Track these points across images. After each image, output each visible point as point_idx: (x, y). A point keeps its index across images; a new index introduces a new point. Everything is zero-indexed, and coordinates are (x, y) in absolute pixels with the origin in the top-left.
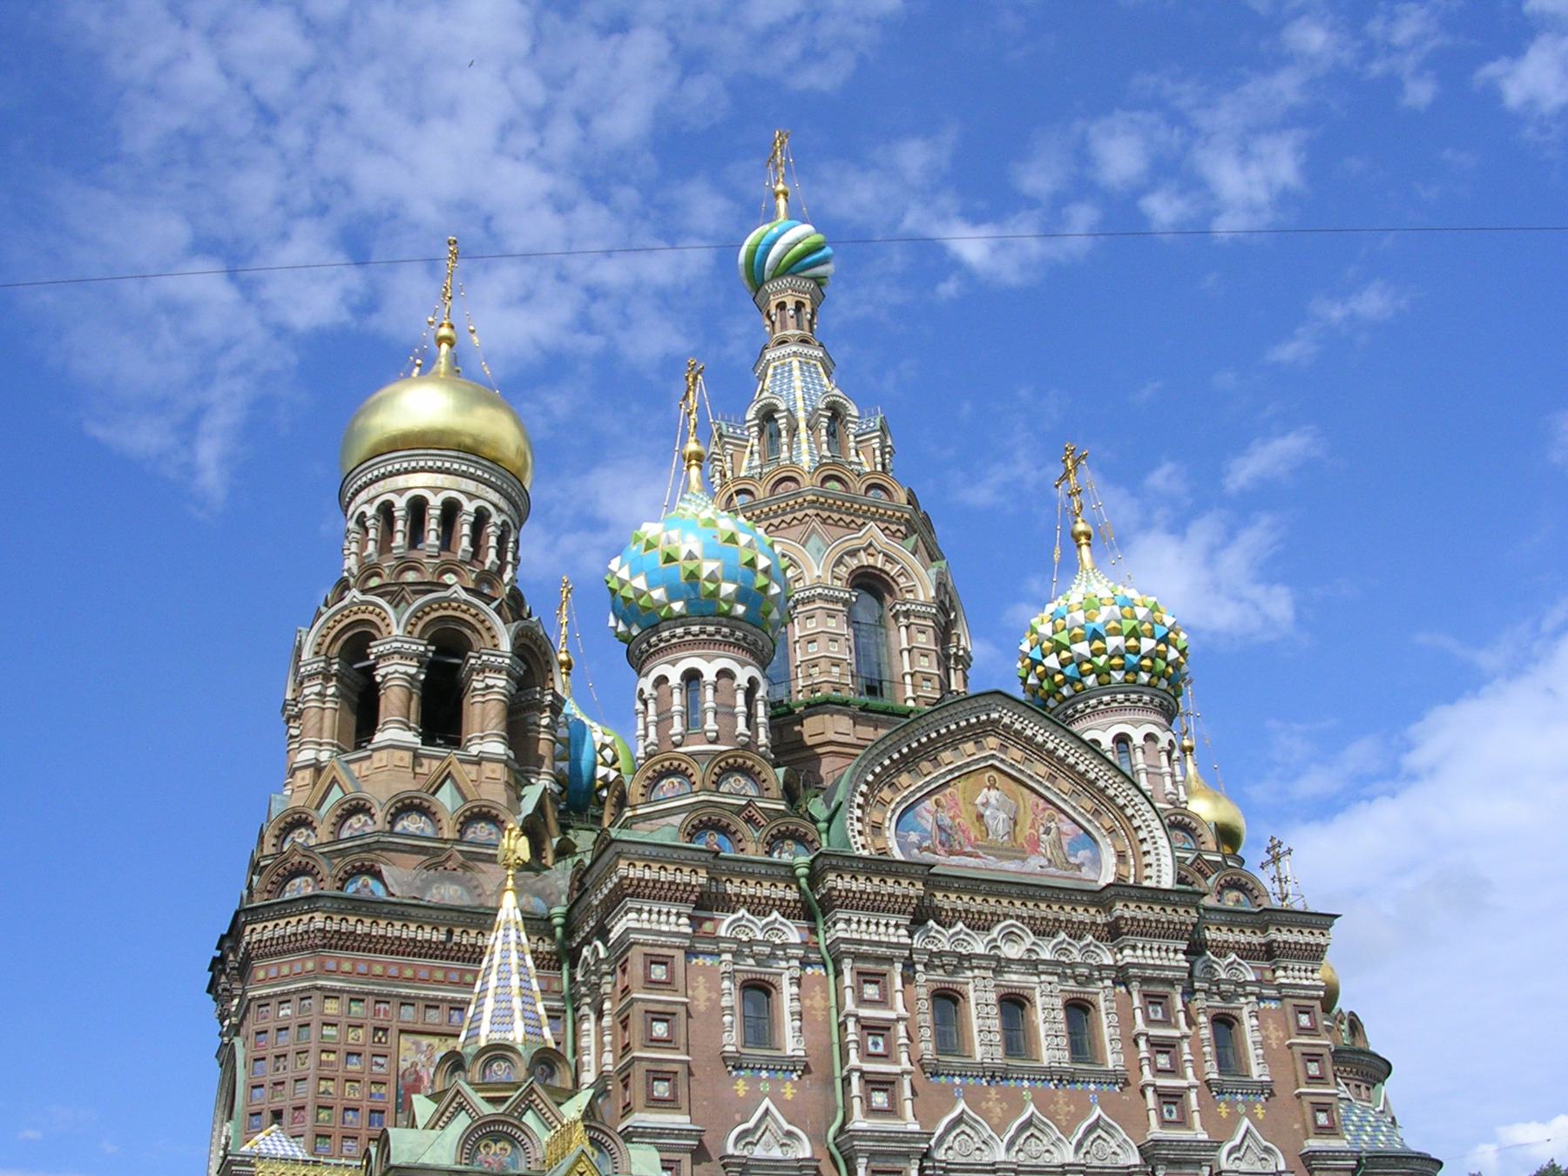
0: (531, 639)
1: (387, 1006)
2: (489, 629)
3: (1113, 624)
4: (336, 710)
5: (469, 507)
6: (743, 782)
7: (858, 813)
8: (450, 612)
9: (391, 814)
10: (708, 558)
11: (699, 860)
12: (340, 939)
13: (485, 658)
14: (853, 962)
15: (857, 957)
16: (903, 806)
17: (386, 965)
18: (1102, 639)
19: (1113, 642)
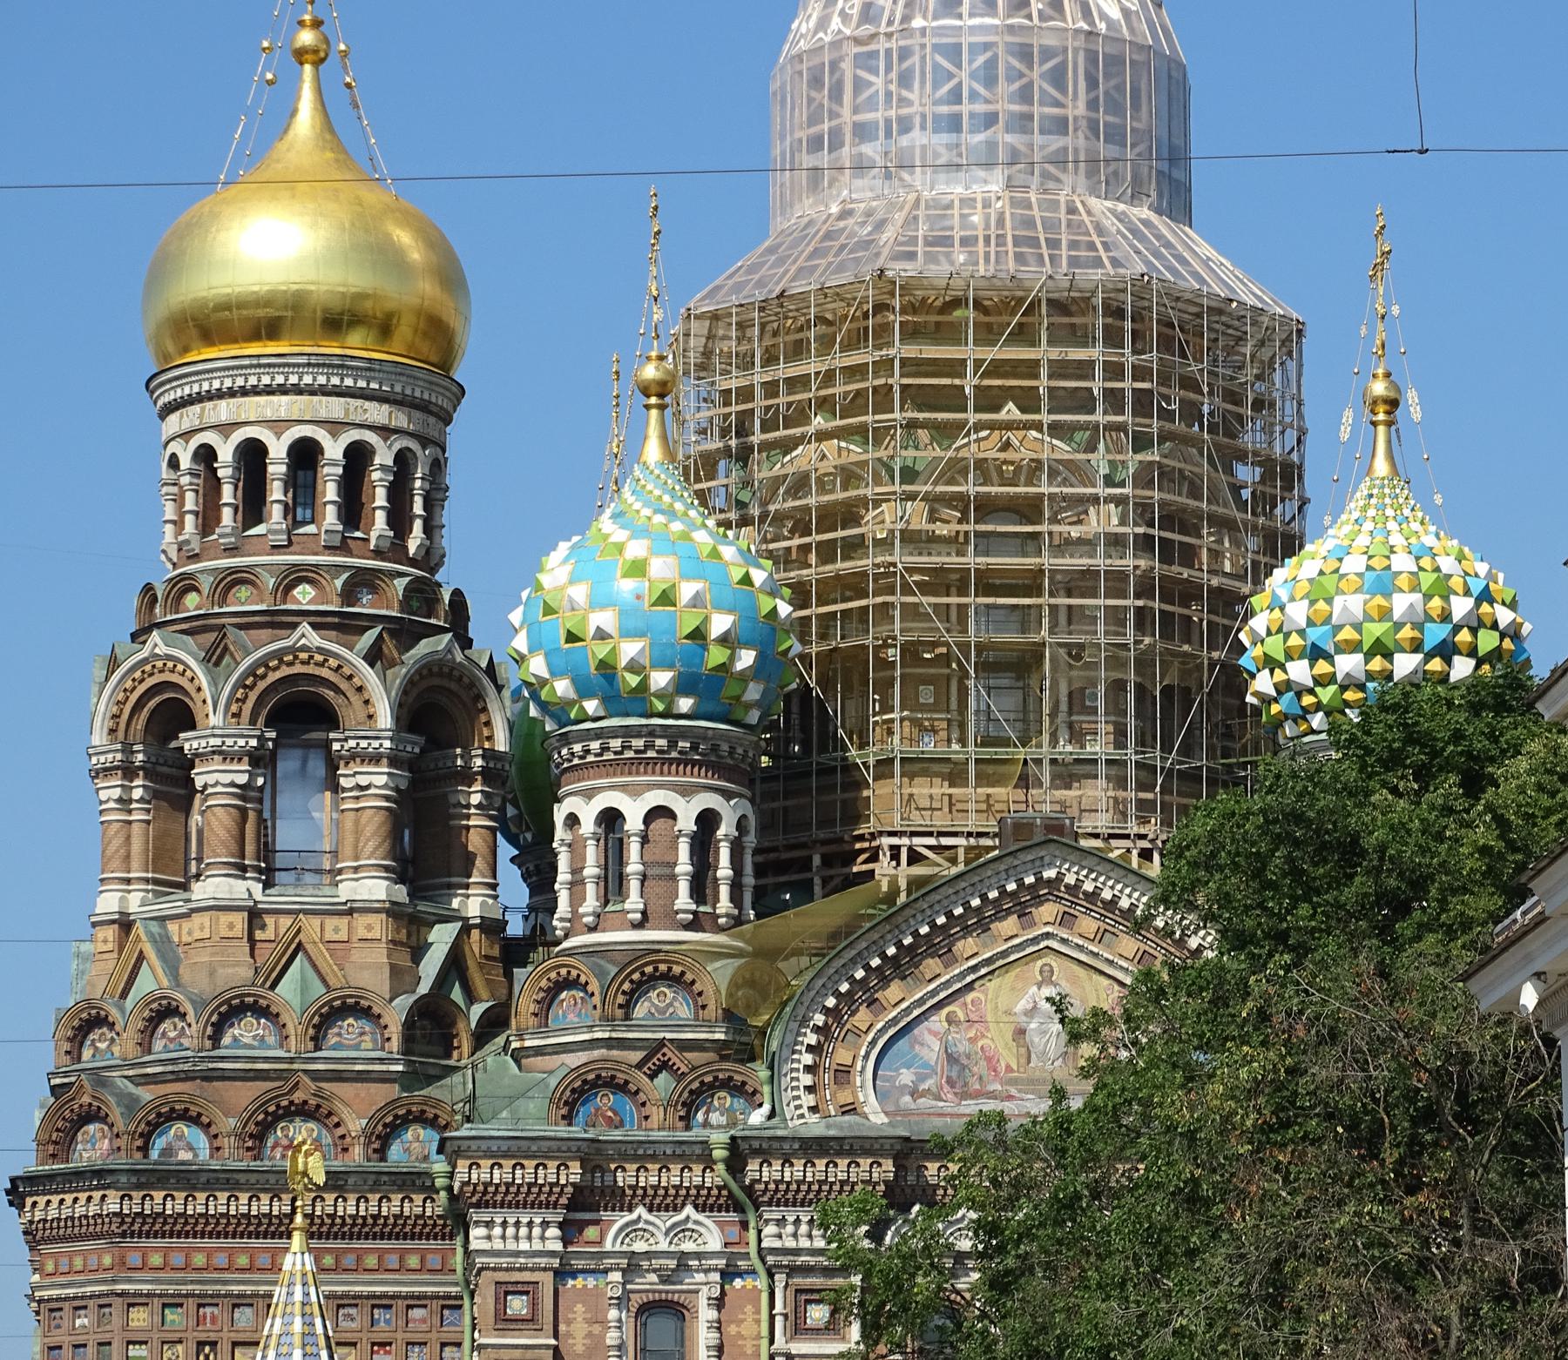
0: (441, 674)
1: (216, 1310)
2: (360, 689)
3: (1347, 634)
4: (148, 822)
5: (334, 449)
6: (670, 995)
7: (808, 1059)
8: (298, 669)
9: (213, 1024)
10: (627, 634)
11: (569, 1150)
12: (143, 1224)
13: (352, 743)
14: (788, 1276)
15: (793, 1271)
16: (891, 1032)
17: (210, 1253)
18: (1329, 658)
19: (1348, 664)
